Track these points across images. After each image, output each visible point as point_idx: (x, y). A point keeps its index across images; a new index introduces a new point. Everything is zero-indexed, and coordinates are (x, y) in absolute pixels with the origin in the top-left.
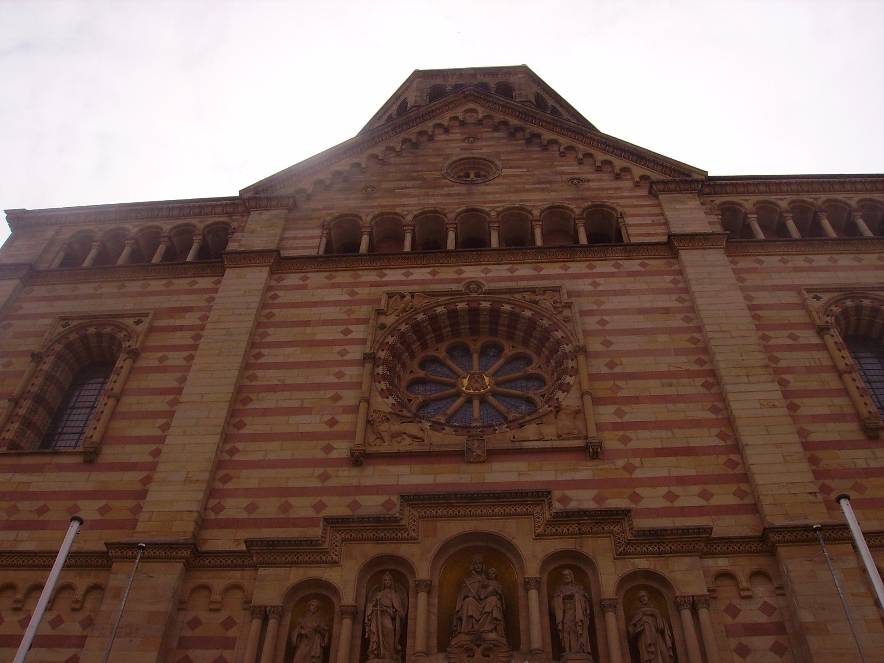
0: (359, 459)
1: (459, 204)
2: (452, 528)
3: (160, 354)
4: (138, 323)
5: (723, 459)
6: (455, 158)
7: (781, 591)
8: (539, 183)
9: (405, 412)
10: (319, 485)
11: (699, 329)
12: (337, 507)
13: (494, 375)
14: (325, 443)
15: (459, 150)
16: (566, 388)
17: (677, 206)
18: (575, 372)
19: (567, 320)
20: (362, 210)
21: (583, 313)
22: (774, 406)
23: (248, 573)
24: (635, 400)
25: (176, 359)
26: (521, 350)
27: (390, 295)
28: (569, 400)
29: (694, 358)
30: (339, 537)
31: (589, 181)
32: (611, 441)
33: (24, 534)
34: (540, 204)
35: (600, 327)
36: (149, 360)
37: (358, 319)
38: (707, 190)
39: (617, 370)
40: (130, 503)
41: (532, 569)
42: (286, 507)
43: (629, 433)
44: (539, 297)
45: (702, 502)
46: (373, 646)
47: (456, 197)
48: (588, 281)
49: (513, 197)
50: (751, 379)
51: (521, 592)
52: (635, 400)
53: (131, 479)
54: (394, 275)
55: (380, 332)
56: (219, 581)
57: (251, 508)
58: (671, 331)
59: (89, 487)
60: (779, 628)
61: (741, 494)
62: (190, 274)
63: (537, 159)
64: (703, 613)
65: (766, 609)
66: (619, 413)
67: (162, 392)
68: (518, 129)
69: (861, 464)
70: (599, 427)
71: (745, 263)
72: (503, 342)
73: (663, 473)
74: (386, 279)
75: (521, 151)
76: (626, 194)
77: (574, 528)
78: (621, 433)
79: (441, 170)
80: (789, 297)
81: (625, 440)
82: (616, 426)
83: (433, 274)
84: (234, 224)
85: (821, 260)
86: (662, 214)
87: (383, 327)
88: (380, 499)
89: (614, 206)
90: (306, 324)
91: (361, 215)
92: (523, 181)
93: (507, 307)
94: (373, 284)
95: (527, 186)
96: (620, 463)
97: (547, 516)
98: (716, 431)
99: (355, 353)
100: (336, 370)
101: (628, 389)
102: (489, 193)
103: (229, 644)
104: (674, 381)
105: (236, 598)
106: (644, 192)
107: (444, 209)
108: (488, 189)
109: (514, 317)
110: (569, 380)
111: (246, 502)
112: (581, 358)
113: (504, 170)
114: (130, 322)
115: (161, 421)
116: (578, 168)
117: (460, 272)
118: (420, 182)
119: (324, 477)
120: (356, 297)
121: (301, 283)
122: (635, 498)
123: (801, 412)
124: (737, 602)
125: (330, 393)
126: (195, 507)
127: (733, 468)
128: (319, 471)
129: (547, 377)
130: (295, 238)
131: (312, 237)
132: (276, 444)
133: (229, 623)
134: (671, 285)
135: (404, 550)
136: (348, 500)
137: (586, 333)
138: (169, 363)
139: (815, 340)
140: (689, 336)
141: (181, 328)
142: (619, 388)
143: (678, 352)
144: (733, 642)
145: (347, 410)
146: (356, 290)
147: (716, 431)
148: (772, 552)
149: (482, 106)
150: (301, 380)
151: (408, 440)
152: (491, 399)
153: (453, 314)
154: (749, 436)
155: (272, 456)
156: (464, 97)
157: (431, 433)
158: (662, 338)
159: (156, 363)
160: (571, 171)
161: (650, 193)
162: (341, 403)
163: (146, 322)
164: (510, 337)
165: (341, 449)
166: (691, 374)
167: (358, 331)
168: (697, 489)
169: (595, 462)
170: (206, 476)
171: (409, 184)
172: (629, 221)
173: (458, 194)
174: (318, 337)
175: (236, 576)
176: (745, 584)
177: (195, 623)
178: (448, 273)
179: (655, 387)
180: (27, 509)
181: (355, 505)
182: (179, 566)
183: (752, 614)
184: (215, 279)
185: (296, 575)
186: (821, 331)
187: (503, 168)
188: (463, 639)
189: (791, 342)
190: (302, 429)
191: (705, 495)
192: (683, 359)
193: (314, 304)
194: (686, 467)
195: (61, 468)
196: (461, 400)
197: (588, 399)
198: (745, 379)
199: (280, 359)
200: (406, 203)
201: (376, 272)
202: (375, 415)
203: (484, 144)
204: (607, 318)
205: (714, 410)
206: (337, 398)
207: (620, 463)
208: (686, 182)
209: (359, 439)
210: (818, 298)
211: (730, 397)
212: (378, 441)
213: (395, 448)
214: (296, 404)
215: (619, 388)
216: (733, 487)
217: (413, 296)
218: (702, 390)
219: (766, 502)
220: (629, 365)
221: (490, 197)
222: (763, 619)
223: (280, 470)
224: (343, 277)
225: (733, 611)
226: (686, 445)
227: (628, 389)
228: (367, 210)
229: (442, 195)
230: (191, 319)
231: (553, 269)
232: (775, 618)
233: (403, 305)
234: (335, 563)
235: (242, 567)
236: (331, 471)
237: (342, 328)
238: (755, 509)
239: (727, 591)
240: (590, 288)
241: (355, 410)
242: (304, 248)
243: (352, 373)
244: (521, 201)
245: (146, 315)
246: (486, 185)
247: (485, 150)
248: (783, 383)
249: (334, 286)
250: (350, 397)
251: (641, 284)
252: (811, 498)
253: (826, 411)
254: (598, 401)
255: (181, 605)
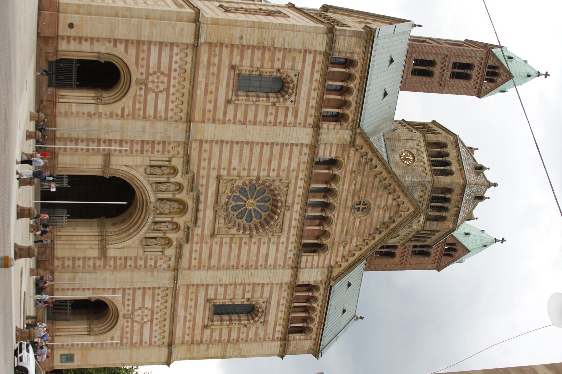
0: (218, 177)
1: (340, 204)
2: (190, 203)
3: (274, 113)
4: (292, 102)
5: (206, 264)
6: (372, 203)
7: (164, 270)
8: (347, 231)
9: (234, 189)
10: (211, 167)
11: (256, 268)
12: (203, 173)
13: (255, 209)
14: (227, 168)
15: (379, 203)
16: (238, 230)
17: (319, 274)
18: (244, 232)
19: (267, 233)
20: (344, 170)
21: (269, 239)
22: (220, 281)
23: (182, 155)
24: (230, 247)
25: (271, 118)
26: (263, 217)
27: (288, 184)
28: (234, 231)
29: (244, 265)
30: (190, 177)
31: (344, 247)
32: (215, 240)
33: (203, 90)
34: (333, 230)
35: (262, 242)
36: (272, 110)
37: (279, 173)
38: (327, 284)
39: (243, 245)
40: (211, 117)
41: (175, 220)
42: (205, 160)
43: (218, 245)
44: (278, 227)
45: (194, 256)
46: (159, 185)
47: (344, 203)
48: (285, 241)
49: (339, 222)
50: (231, 278)
51: (171, 216)
52: (230, 247)
53: (220, 115)
54: (301, 183)
55: (272, 180)
56: (181, 149)
57: (206, 151)
58: (257, 261)
59: (218, 104)
60: (156, 267)
61: (194, 267)
62: (316, 114)
63: (364, 231)
64: (160, 253)
65: (161, 266)
66: (226, 243)
67: (256, 117)
68: (387, 227)
69: (199, 295)
70: (222, 238)
71: (284, 287)
72: (268, 212)
73: (204, 250)
74: (299, 181)
75: (371, 226)
76: (333, 258)
77: (186, 230)
78: (219, 242)
79: (365, 197)
80: (266, 294)
81: (216, 243)
82: (221, 243)
83: (299, 196)
84: (345, 125)
85: (283, 308)
86: (318, 267)
87: (274, 181)
88: (205, 184)
89: (326, 254)
90: (281, 156)
91: (340, 170)
92: (350, 226)
93: (276, 217)
94: (297, 178)
95: (345, 227)
96: (209, 241)
97: (190, 225)
98: (216, 265)
99: (263, 174)
100: (257, 168)
101: (235, 247)
102: (344, 213)
103: (163, 153)
104: (236, 258)
105: (176, 153)
106: (332, 263)
107: (337, 198)
108: (347, 214)
109: (272, 218)
110: (241, 232)
111: (208, 149)
112: (248, 236)
113: (359, 220)
114: (292, 98)
115: (242, 120)
116: (354, 244)
117: (298, 204)
118: (358, 189)
119: (214, 169)
120: (291, 172)
121: (303, 153)
122: (197, 243)
123: (219, 287)
124: (163, 260)
125: (246, 167)
126: (205, 138)
127: (203, 267)
128: (216, 167)
129: (250, 224)
130: (331, 148)
131: (330, 154)
132: (228, 154)
133: (169, 152)
134: (278, 264)
135: (185, 191)
136: (205, 175)
137: (260, 239)
138: (269, 116)
139: (246, 297)
140: (254, 265)
141: (286, 116)
142: (236, 244)
143: (248, 262)
144: (153, 257)
145: (239, 173)
146: (295, 172)
147: (216, 265)
148: (174, 270)
149: (409, 214)
150: (253, 158)
151: (224, 190)
152: (244, 208)
153: (277, 201)
154: (211, 273)
155: (223, 154)
156: (416, 208)
157: (226, 196)
158: (254, 258)
159: (270, 111)
160: (352, 242)
161: (331, 266)
162: (242, 171)
163: (292, 105)
164: (269, 215)
165: (224, 173)
166: (238, 263)
167: (273, 174)
168: (198, 257)
169: (210, 235)
170: (216, 139)
171: (358, 186)
172: (316, 257)
173: (346, 203)
174: (273, 162)
175: (182, 152)
176: (167, 263)
177: (169, 144)
178: (298, 200)
179: (235, 252)
180: (212, 88)
181: (203, 177)
182: (184, 140)
183: (160, 263)
184: (312, 124)
185: (180, 168)
186: (248, 300)
187: (361, 220)
188: (158, 206)
189: (247, 290)
190: (233, 162)
191: (195, 259)
192: (245, 262)
193: (290, 158)
194: (205, 256)
195: (227, 93)
196: (245, 199)
197: (232, 236)
198: (231, 276)
199: (264, 151)
200: (345, 186)
201: (303, 177)
202: (234, 181)
203: (381, 213)
204: (266, 244)
205: (223, 266)
206: (244, 169)
207: (209, 241)
208: (330, 278)
209: (224, 178)
210: (264, 302)
211: (225, 271)
212: (225, 182)
213: (220, 186)
214: (243, 158)
215: (236, 244)
216: (197, 265)
217: (287, 190)
218: (231, 264)
219: (189, 272)
220: (245, 248)
221: (341, 215)
222: (158, 264)
223: (218, 157)
224: (303, 167)
225: (161, 259)
226: (212, 256)
227: (235, 247)
228: (344, 172)
229: (347, 198)
230: (290, 118)
231: (293, 231)
232: (158, 267)
233: (282, 187)
234: (182, 177)
235: (184, 154)
236: (216, 170)
237: (276, 168)
238: (189, 268)
239: (167, 259)
240: (281, 241)
241: (239, 175)
242: (324, 152)
243: (255, 173)
244: (336, 224)
245: (294, 104)
246: (350, 213)
247: (376, 214)
248: (231, 285)
249: (299, 165)
250: (244, 173)
251: (281, 256)
252: (189, 282)
253: (219, 292)
254: (231, 239)
255: (174, 142)
